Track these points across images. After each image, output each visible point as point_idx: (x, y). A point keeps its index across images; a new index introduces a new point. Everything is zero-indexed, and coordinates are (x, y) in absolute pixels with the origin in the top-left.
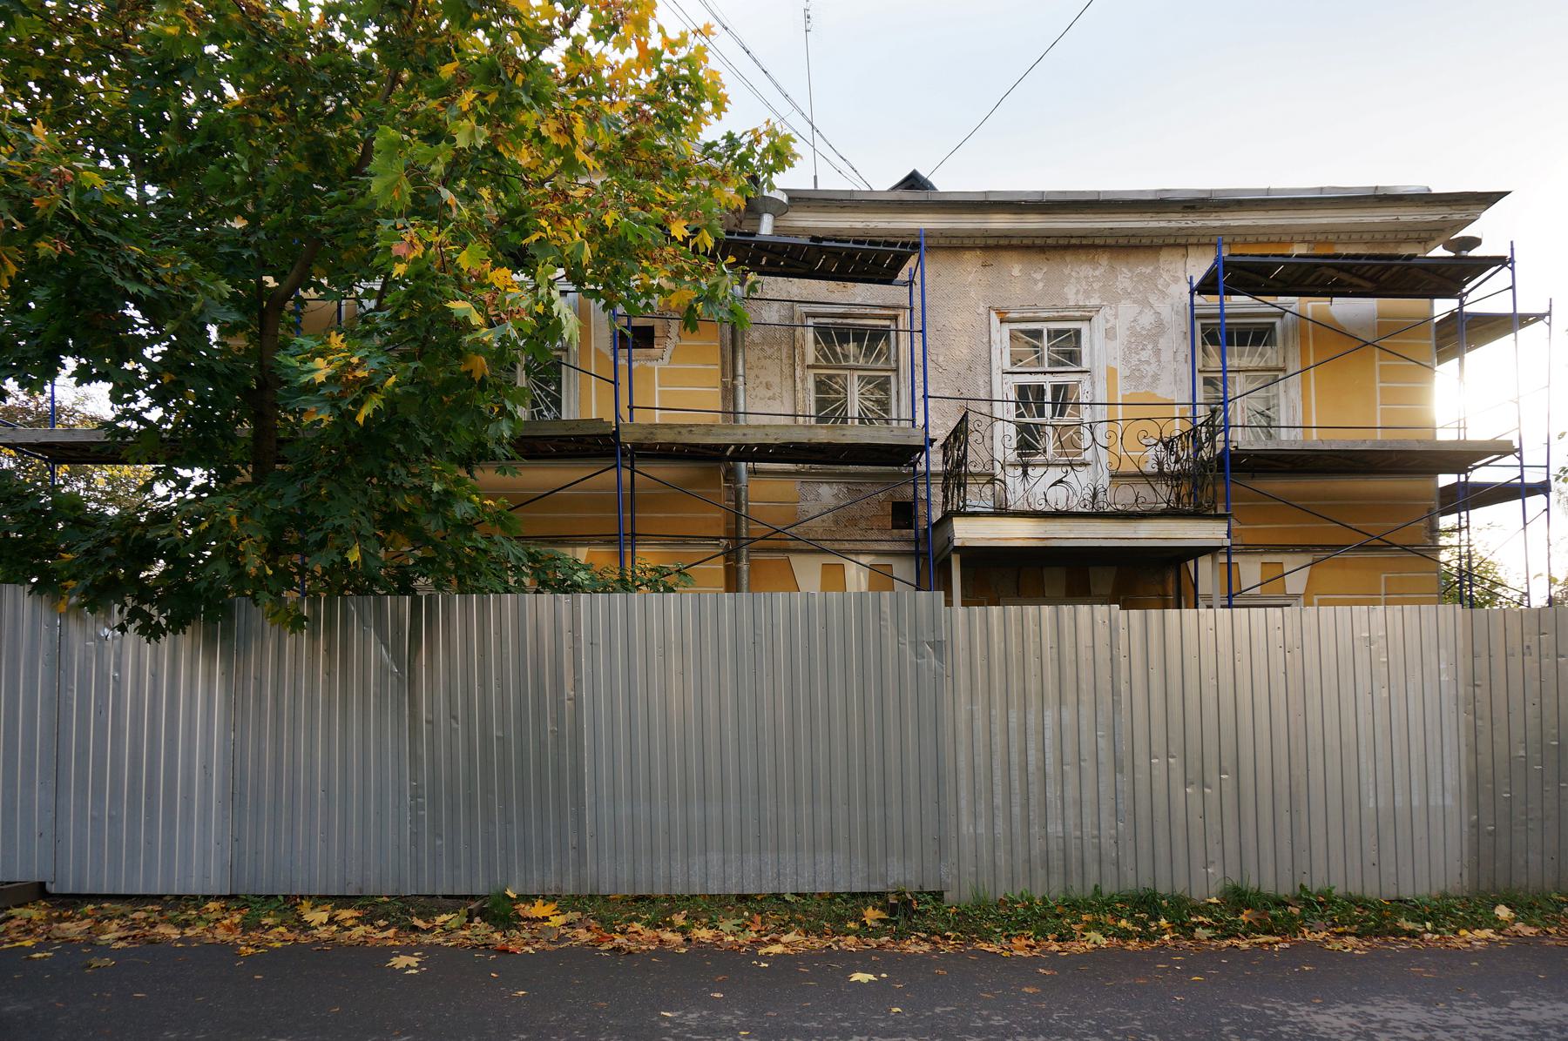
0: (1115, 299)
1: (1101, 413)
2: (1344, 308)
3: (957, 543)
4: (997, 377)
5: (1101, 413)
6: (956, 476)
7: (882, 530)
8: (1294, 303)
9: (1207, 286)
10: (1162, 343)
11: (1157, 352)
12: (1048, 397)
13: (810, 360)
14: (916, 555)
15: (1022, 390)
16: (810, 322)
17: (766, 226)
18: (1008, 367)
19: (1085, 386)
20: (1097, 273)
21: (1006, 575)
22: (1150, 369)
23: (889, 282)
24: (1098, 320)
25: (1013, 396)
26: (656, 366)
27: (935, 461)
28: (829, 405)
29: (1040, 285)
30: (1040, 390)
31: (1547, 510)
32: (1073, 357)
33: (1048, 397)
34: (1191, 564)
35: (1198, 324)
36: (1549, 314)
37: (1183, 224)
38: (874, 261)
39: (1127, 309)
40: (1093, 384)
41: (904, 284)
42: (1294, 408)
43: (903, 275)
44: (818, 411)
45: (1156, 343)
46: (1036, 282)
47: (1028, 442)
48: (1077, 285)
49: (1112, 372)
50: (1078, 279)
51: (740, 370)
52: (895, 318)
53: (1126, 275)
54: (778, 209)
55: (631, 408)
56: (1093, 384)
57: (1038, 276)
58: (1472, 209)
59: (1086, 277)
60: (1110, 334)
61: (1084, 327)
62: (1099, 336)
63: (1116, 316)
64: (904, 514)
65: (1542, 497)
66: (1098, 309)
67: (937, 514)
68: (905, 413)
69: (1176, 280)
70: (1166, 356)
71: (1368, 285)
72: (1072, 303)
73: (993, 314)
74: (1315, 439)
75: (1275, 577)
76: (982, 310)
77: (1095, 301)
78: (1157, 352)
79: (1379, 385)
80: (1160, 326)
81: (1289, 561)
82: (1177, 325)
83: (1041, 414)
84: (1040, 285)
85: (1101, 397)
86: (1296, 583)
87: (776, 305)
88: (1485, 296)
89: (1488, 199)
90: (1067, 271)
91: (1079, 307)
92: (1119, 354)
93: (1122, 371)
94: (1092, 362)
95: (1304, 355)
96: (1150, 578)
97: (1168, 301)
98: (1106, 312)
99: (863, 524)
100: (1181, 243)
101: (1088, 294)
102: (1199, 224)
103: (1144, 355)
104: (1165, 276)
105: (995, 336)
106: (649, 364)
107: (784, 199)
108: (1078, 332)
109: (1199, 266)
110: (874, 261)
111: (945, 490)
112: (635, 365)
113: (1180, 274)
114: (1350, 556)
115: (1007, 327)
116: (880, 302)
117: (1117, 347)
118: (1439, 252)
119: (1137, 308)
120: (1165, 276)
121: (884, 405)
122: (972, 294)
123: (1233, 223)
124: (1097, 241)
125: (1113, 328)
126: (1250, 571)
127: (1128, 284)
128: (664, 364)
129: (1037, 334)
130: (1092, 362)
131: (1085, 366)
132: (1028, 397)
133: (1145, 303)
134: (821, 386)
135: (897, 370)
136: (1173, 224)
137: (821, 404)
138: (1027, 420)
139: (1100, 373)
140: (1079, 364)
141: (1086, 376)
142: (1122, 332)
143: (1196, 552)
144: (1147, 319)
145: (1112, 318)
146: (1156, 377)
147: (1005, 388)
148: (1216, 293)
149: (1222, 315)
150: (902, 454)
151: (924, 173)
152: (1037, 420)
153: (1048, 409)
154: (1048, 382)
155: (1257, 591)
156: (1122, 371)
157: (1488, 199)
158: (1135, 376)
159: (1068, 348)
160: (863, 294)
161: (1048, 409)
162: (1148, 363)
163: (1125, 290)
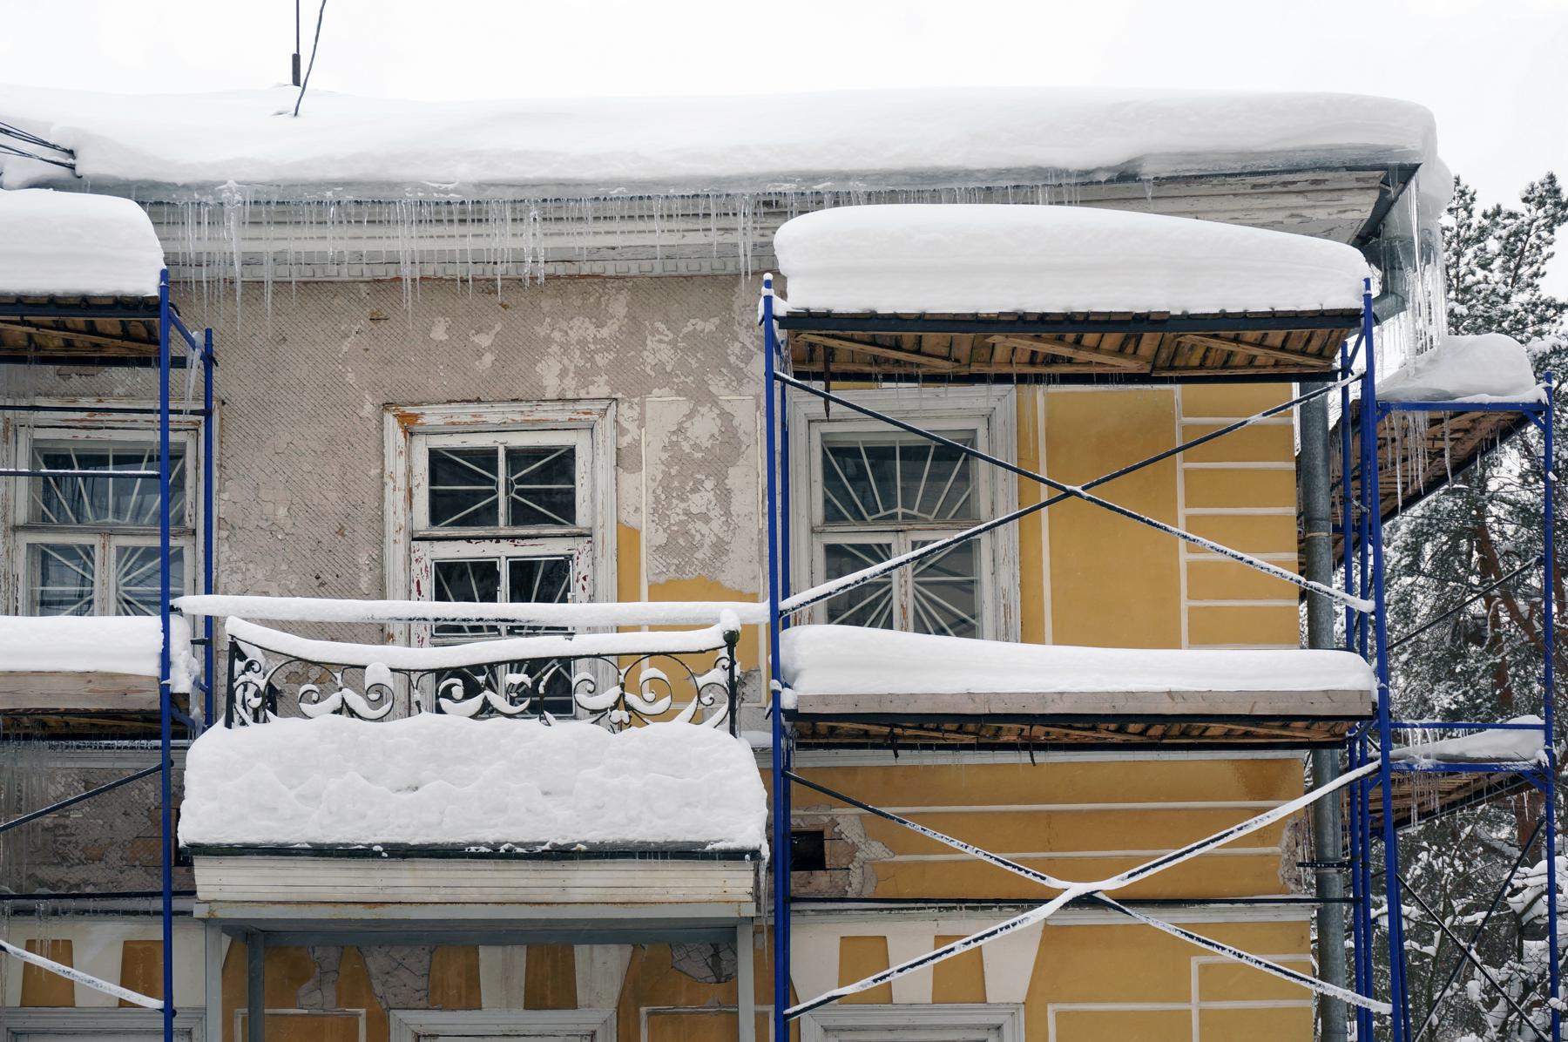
11: (724, 496)
19: (579, 568)
24: (605, 428)
29: (488, 358)
32: (564, 508)
39: (664, 407)
49: (628, 538)
50: (565, 348)
57: (484, 340)
76: (368, 409)
80: (730, 439)
84: (488, 358)
92: (646, 501)
94: (593, 518)
103: (698, 503)
105: (395, 464)
117: (640, 486)
119: (685, 406)
127: (666, 354)
129: (487, 458)
130: (593, 518)
133: (701, 396)
144: (704, 428)
146: (720, 548)
154: (502, 553)
162: (705, 518)
163: (660, 368)
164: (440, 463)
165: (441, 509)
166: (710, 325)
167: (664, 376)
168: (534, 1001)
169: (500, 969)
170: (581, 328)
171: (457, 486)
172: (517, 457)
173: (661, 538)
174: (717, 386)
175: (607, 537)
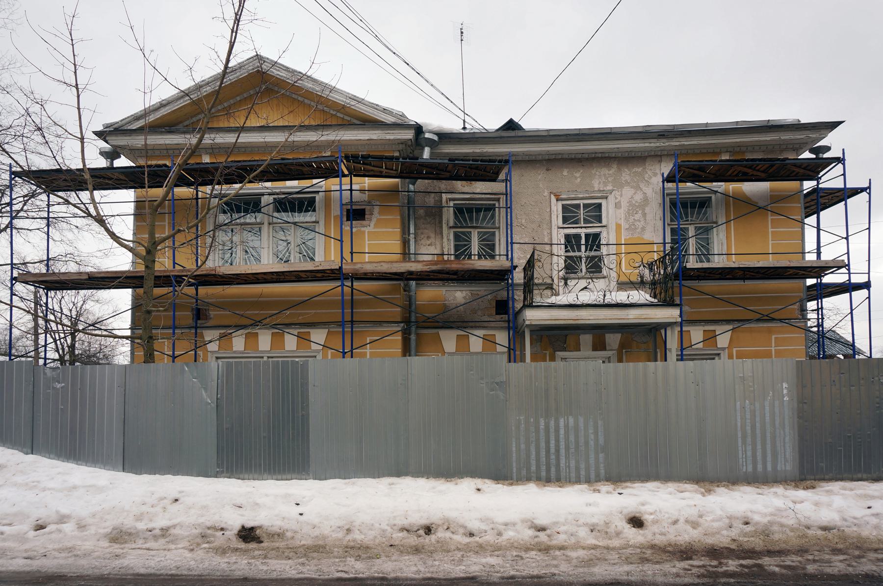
0: (621, 186)
1: (613, 249)
2: (750, 188)
3: (527, 323)
4: (555, 231)
5: (613, 249)
6: (529, 286)
7: (489, 316)
8: (720, 186)
9: (670, 179)
10: (647, 210)
11: (644, 215)
12: (583, 241)
13: (451, 224)
14: (509, 329)
15: (568, 237)
16: (451, 204)
17: (426, 154)
18: (561, 225)
20: (611, 172)
21: (557, 339)
22: (640, 225)
23: (494, 180)
25: (563, 241)
26: (367, 230)
27: (518, 277)
28: (462, 248)
29: (579, 180)
30: (577, 237)
31: (869, 298)
33: (583, 241)
34: (663, 332)
35: (667, 200)
36: (869, 188)
37: (658, 145)
38: (486, 169)
39: (628, 192)
40: (608, 233)
41: (503, 181)
42: (722, 244)
43: (502, 176)
44: (456, 250)
45: (643, 210)
46: (576, 178)
47: (571, 267)
48: (598, 180)
49: (618, 227)
51: (412, 230)
52: (498, 200)
53: (626, 174)
54: (431, 143)
55: (352, 253)
56: (608, 233)
57: (578, 175)
58: (823, 132)
59: (605, 175)
60: (618, 205)
61: (604, 202)
62: (612, 206)
63: (621, 196)
64: (502, 307)
65: (865, 291)
66: (611, 192)
67: (519, 305)
68: (503, 252)
69: (655, 175)
70: (649, 217)
71: (763, 175)
72: (596, 189)
73: (552, 196)
74: (734, 262)
75: (710, 338)
76: (546, 194)
77: (609, 188)
78: (644, 215)
79: (770, 230)
80: (646, 200)
81: (719, 329)
82: (655, 201)
83: (580, 250)
84: (579, 180)
85: (613, 240)
86: (723, 341)
87: (433, 195)
88: (831, 179)
89: (833, 125)
90: (593, 172)
91: (600, 191)
92: (623, 216)
93: (624, 225)
94: (608, 222)
95: (727, 215)
96: (641, 341)
97: (651, 186)
98: (616, 193)
99: (479, 313)
100: (658, 156)
101: (605, 184)
102: (667, 144)
103: (637, 217)
104: (649, 172)
105: (554, 208)
106: (362, 229)
107: (436, 138)
108: (600, 205)
109: (666, 168)
110: (486, 169)
111: (524, 292)
112: (354, 230)
113: (658, 171)
114: (752, 325)
115: (560, 204)
116: (490, 191)
117: (622, 212)
118: (807, 155)
119: (633, 191)
120: (649, 172)
121: (492, 247)
122: (541, 185)
123: (686, 143)
124: (610, 155)
125: (620, 202)
126: (696, 334)
127: (628, 178)
128: (371, 228)
129: (577, 206)
130: (608, 222)
131: (604, 222)
132: (571, 242)
133: (638, 188)
134: (457, 237)
135: (499, 228)
136: (652, 145)
137: (457, 247)
138: (571, 254)
139: (612, 227)
140: (600, 222)
141: (604, 229)
142: (624, 204)
143: (665, 326)
144: (639, 197)
145: (619, 197)
146: (643, 229)
147: (559, 236)
148: (674, 181)
149: (677, 194)
150: (502, 275)
151: (516, 120)
152: (577, 254)
153: (583, 248)
154: (583, 232)
155: (701, 345)
156: (624, 225)
157: (833, 125)
158: (632, 228)
159: (595, 212)
160: (481, 187)
161: (583, 248)
162: (639, 221)
163: (626, 181)
164: (564, 208)
165: (565, 220)
166: (640, 170)
167: (627, 183)
168: (595, 349)
169: (586, 339)
170: (605, 171)
171: (569, 215)
172: (586, 206)
173: (627, 226)
174: (642, 185)
175: (612, 227)
